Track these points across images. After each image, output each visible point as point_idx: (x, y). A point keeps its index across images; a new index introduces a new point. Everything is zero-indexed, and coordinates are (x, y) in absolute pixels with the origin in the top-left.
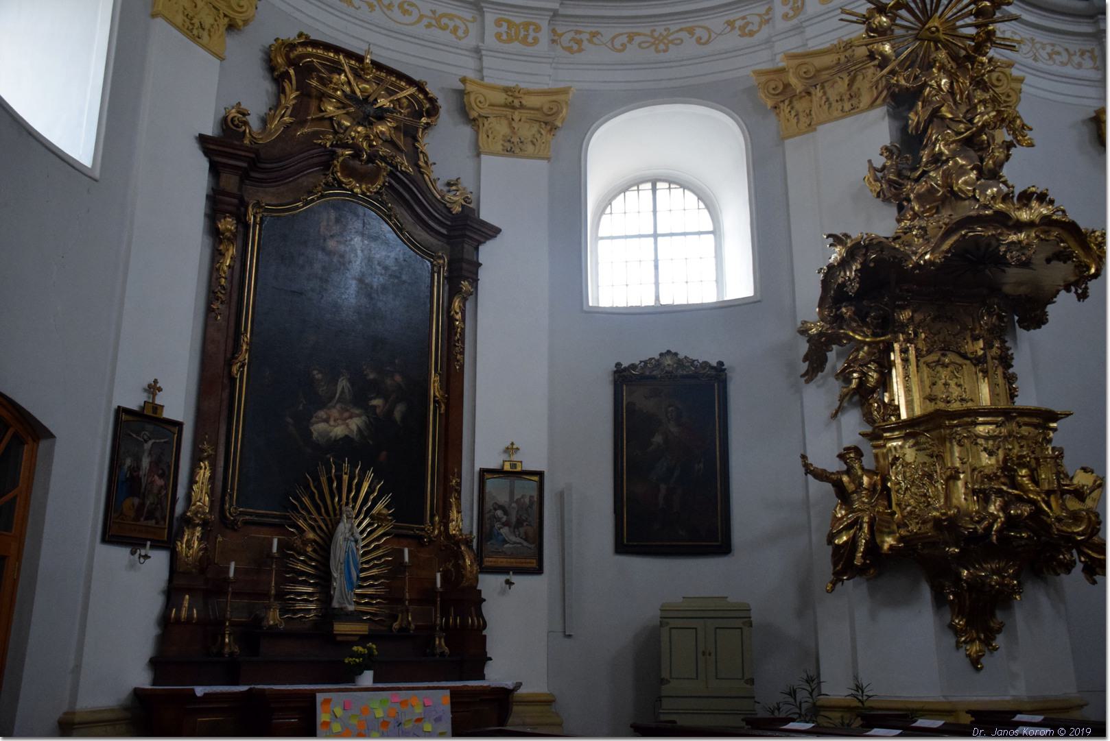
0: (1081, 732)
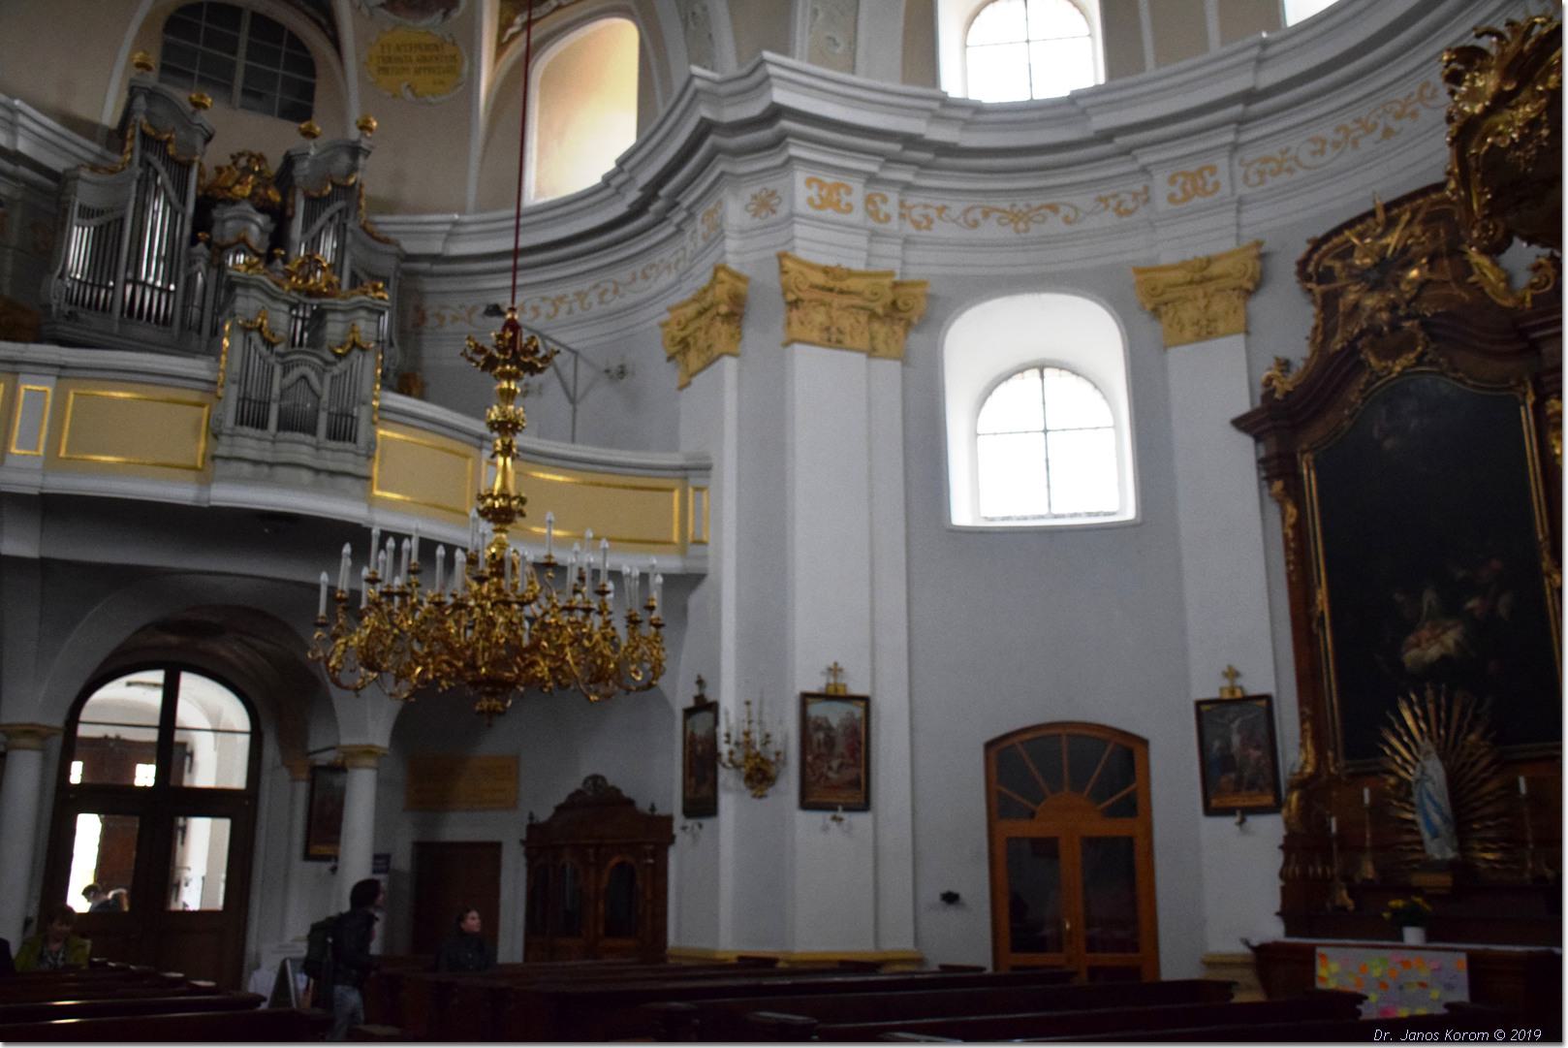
0: (1527, 1035)
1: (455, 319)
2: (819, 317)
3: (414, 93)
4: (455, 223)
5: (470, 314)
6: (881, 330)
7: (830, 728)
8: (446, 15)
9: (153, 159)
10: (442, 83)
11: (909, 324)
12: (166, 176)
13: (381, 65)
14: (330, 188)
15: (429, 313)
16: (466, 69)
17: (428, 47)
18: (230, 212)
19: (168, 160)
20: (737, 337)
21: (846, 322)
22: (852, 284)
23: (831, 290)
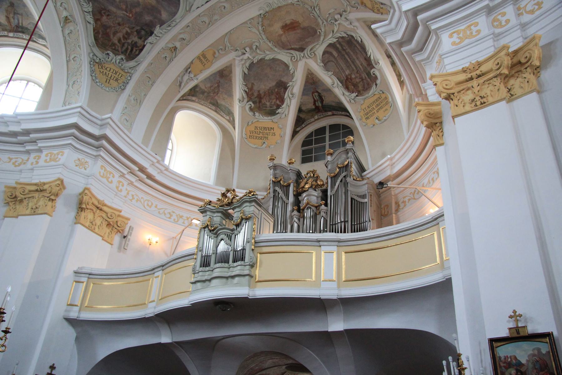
1: (409, 200)
2: (469, 96)
3: (379, 120)
4: (391, 159)
5: (413, 195)
6: (515, 83)
7: (520, 364)
8: (376, 85)
9: (277, 188)
10: (386, 110)
11: (537, 70)
12: (282, 192)
13: (366, 117)
14: (338, 170)
15: (400, 203)
16: (390, 100)
17: (376, 100)
18: (304, 195)
19: (282, 187)
20: (441, 134)
21: (487, 90)
22: (484, 68)
23: (471, 79)
